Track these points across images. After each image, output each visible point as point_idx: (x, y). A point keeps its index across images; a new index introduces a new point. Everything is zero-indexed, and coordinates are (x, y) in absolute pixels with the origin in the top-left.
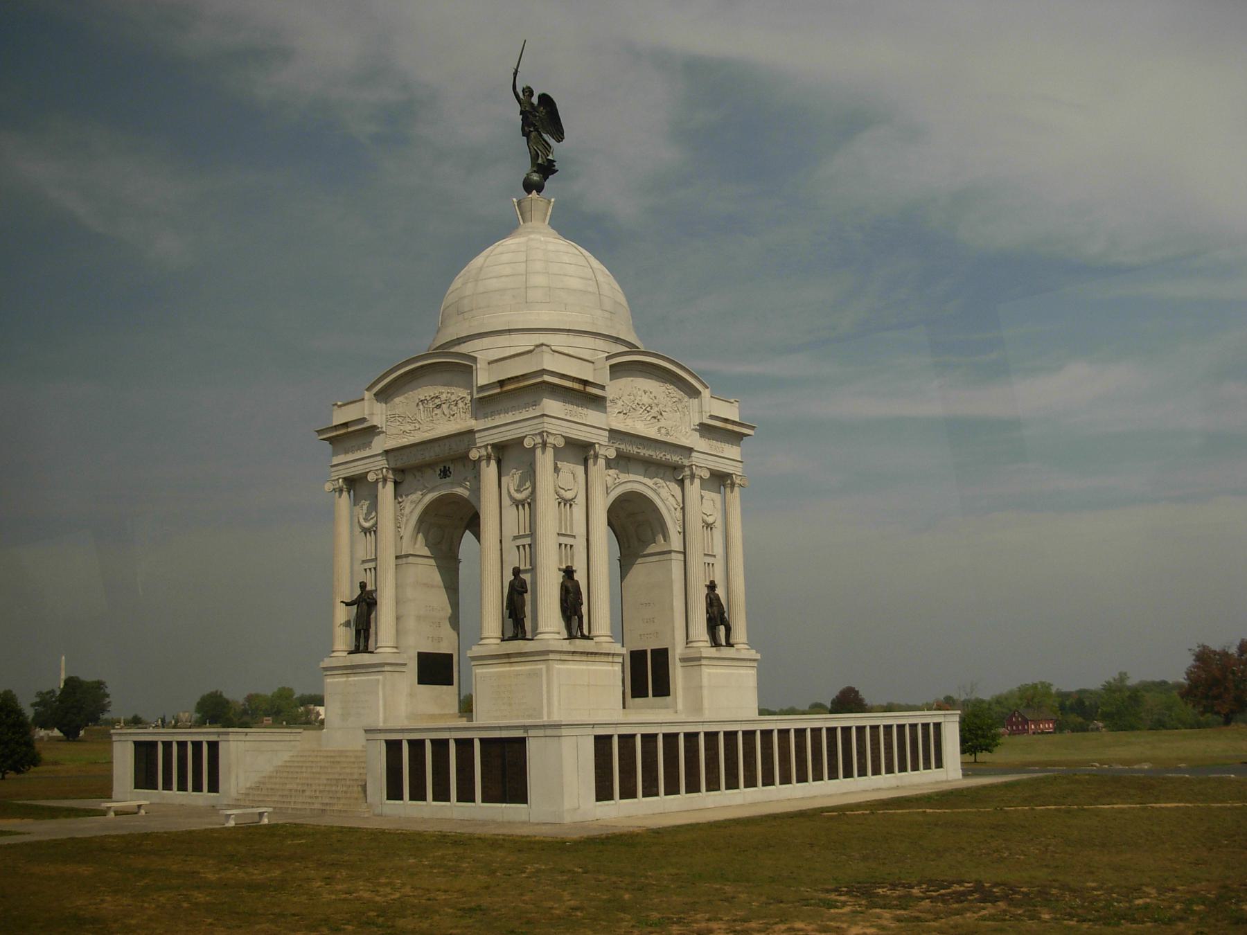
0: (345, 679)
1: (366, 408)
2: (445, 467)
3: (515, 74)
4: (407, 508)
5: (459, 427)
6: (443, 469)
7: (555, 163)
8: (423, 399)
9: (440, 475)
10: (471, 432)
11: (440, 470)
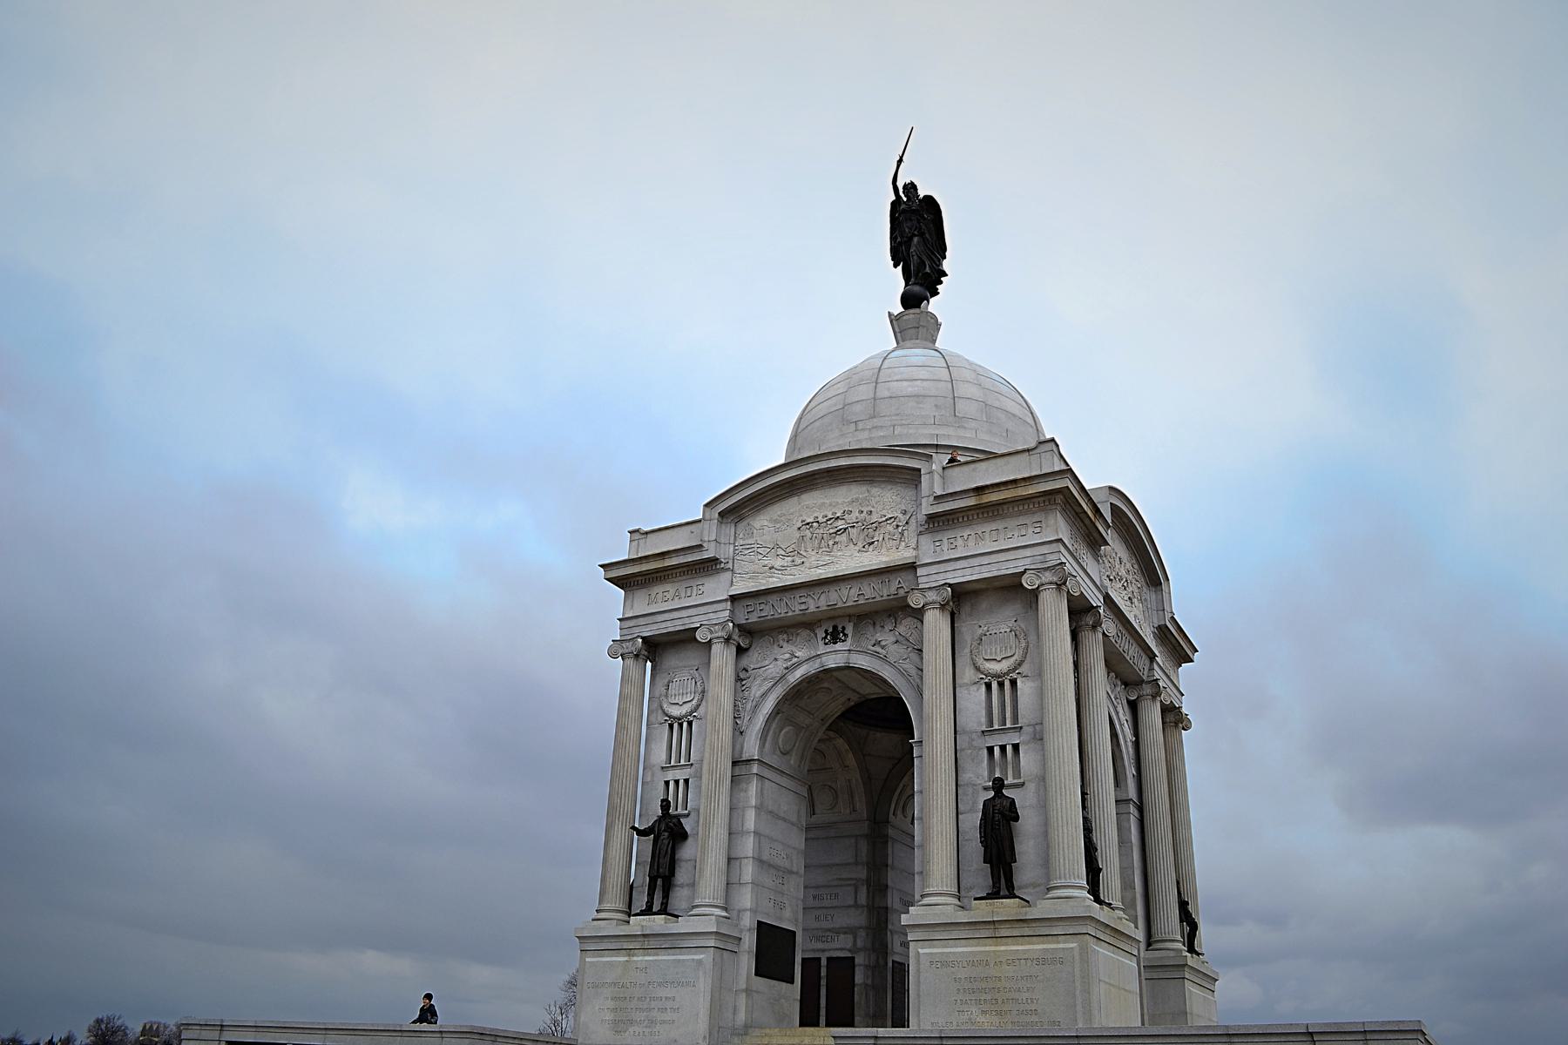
0: (626, 959)
1: (706, 532)
2: (835, 628)
3: (900, 161)
4: (754, 689)
5: (884, 559)
6: (830, 630)
7: (942, 279)
8: (812, 520)
9: (826, 638)
10: (911, 567)
11: (826, 631)
